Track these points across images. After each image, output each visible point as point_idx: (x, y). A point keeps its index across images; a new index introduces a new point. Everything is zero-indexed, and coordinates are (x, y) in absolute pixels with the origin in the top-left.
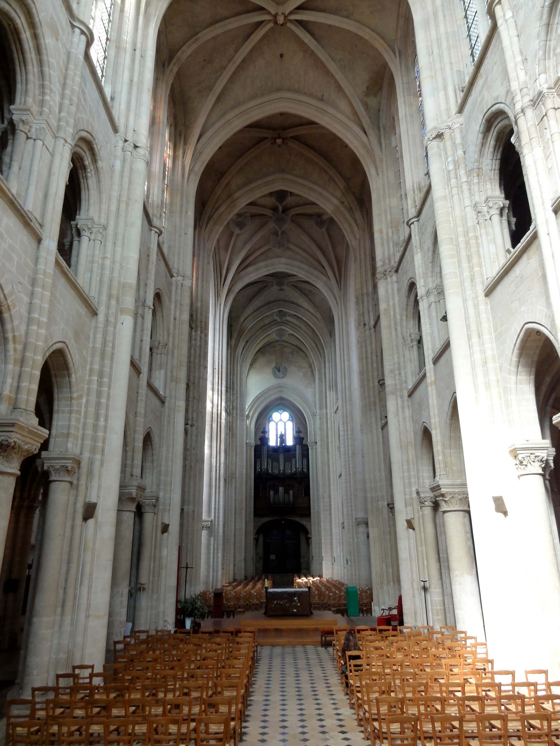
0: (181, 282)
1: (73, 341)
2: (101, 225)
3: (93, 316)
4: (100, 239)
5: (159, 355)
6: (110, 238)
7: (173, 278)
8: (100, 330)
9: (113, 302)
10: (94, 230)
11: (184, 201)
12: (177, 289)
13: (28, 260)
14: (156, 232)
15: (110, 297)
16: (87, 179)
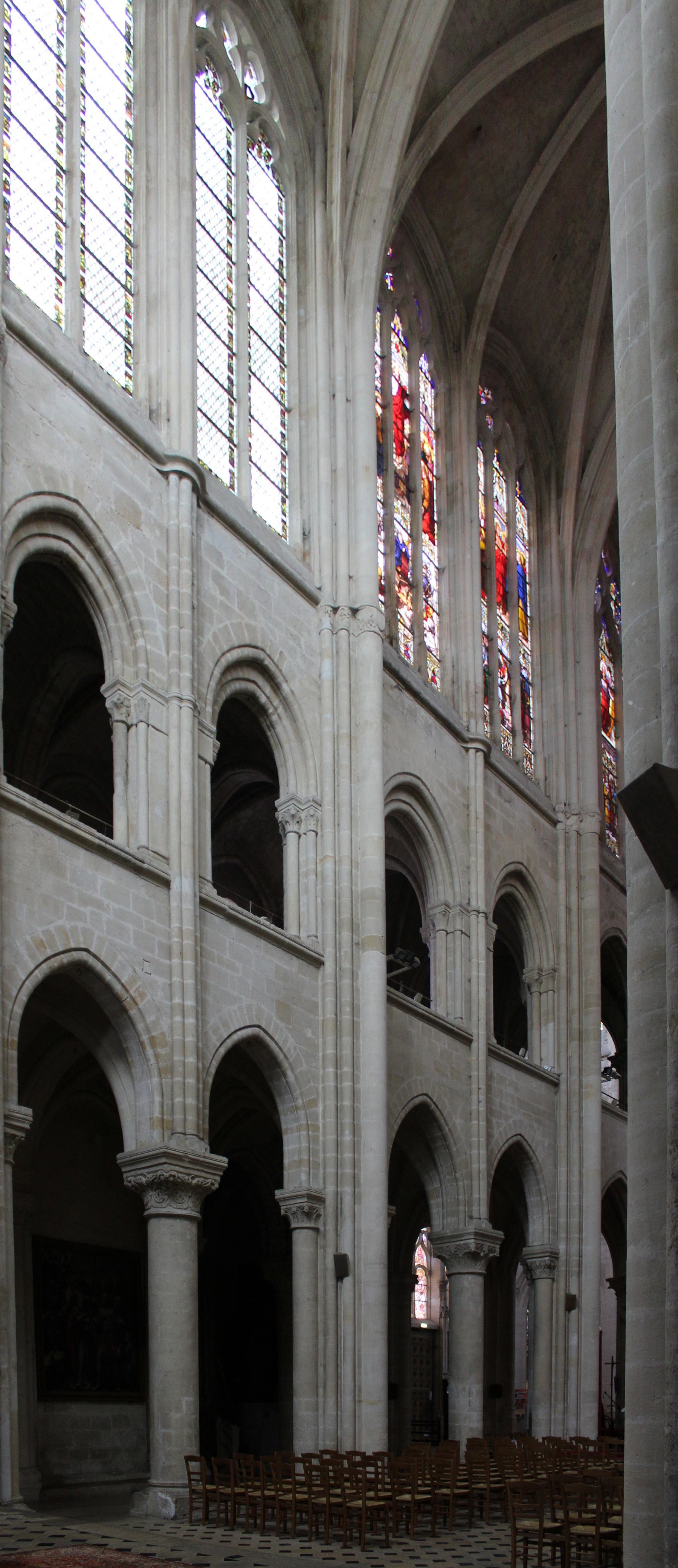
0: (575, 827)
1: (275, 1020)
2: (309, 801)
3: (318, 968)
4: (312, 827)
5: (544, 996)
6: (328, 819)
7: (559, 826)
8: (330, 989)
9: (346, 934)
10: (303, 815)
11: (570, 634)
12: (567, 846)
13: (154, 921)
14: (477, 750)
15: (337, 925)
16: (274, 728)
